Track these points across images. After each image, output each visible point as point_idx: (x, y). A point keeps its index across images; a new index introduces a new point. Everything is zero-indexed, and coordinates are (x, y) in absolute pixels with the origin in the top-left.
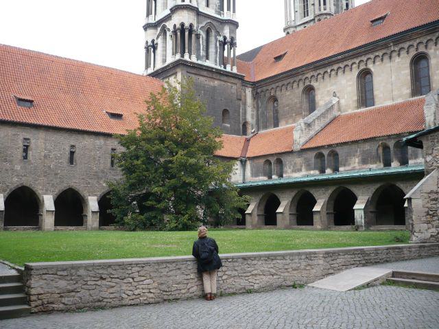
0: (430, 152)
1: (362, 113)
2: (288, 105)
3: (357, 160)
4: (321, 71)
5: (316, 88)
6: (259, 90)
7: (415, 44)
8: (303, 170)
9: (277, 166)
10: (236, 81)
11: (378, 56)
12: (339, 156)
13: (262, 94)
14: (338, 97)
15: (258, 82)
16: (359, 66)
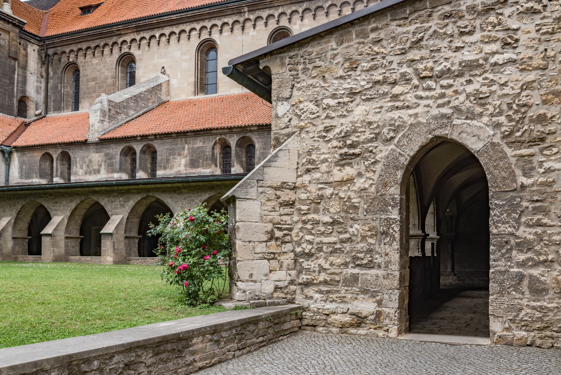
0: (286, 94)
1: (200, 101)
2: (94, 79)
3: (183, 161)
4: (147, 35)
5: (137, 58)
6: (50, 52)
7: (276, 15)
8: (103, 170)
9: (62, 164)
10: (8, 27)
11: (226, 23)
12: (158, 153)
13: (56, 57)
14: (168, 76)
15: (49, 38)
16: (200, 34)
